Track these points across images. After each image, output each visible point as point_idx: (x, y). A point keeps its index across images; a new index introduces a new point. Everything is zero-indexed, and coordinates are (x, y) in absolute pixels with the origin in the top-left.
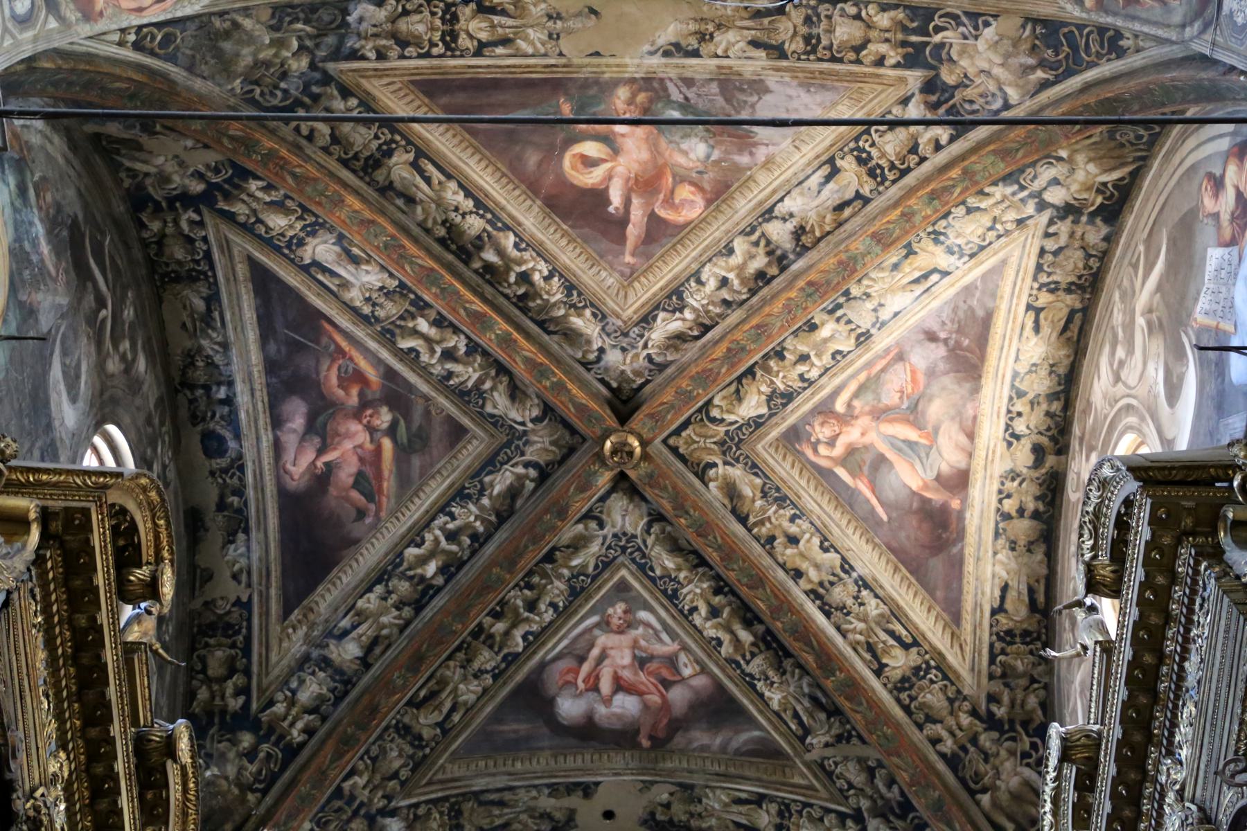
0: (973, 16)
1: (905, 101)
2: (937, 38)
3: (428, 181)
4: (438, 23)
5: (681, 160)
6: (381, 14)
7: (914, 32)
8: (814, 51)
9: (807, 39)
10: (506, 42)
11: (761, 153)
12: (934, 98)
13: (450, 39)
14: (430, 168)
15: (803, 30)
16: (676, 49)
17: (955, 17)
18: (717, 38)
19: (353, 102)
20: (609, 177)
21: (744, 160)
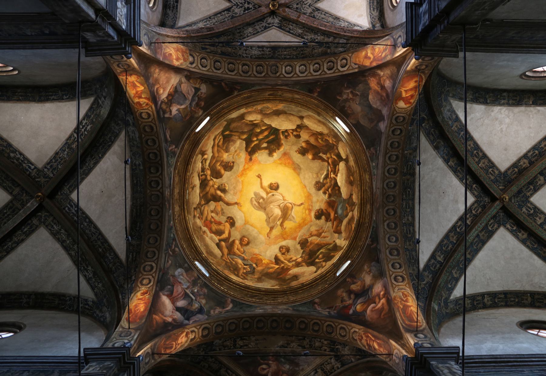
0: (344, 344)
1: (331, 359)
2: (337, 347)
3: (229, 374)
4: (232, 342)
5: (284, 369)
6: (221, 342)
7: (333, 345)
8: (311, 347)
9: (310, 345)
10: (246, 345)
11: (301, 368)
12: (337, 358)
13: (235, 346)
14: (229, 372)
15: (309, 343)
16: (282, 346)
17: (340, 344)
18: (291, 344)
19: (213, 359)
20: (268, 372)
21: (297, 369)
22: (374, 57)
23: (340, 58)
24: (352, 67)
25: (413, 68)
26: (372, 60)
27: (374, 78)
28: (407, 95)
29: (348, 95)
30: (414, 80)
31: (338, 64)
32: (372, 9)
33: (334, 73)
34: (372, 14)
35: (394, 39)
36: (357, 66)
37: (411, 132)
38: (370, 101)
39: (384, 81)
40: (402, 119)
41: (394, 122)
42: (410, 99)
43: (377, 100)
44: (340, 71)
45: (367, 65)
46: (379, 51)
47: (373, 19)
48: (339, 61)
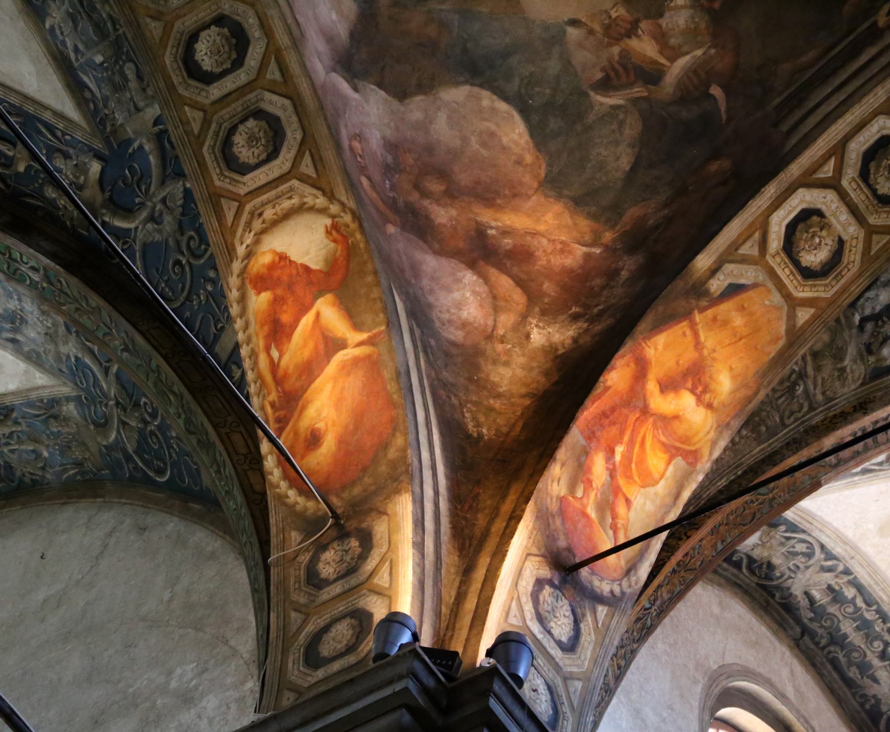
22: (645, 411)
23: (853, 257)
24: (745, 260)
25: (380, 529)
26: (652, 386)
27: (569, 271)
28: (307, 320)
29: (661, 37)
30: (328, 445)
31: (844, 216)
32: (850, 593)
33: (839, 150)
34: (830, 570)
35: (597, 599)
36: (716, 285)
37: (133, 84)
38: (502, 106)
39: (496, 302)
40: (244, 152)
41: (275, 104)
42: (277, 301)
43: (465, 139)
44: (807, 181)
45: (661, 339)
46: (642, 461)
47: (801, 548)
48: (850, 230)
